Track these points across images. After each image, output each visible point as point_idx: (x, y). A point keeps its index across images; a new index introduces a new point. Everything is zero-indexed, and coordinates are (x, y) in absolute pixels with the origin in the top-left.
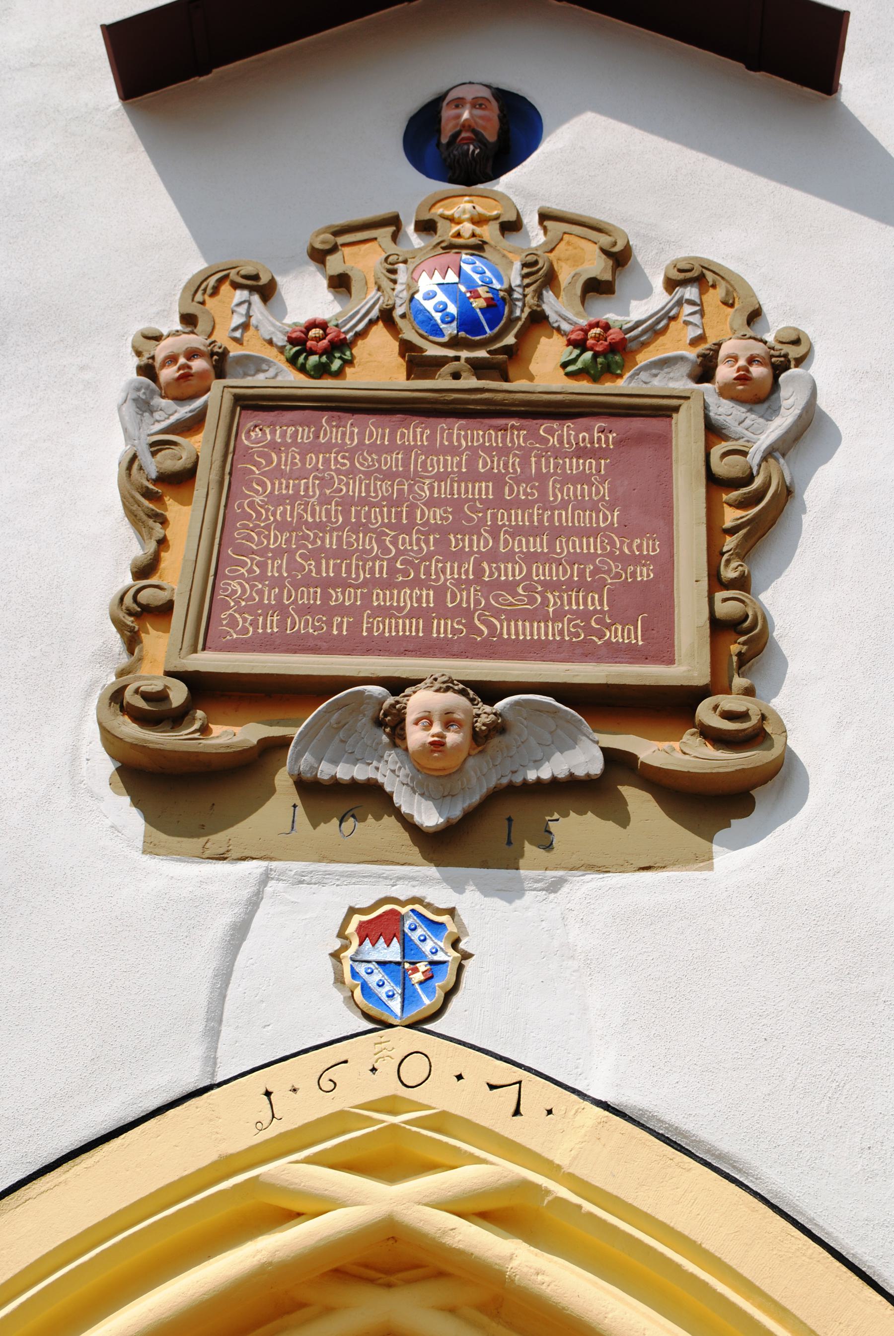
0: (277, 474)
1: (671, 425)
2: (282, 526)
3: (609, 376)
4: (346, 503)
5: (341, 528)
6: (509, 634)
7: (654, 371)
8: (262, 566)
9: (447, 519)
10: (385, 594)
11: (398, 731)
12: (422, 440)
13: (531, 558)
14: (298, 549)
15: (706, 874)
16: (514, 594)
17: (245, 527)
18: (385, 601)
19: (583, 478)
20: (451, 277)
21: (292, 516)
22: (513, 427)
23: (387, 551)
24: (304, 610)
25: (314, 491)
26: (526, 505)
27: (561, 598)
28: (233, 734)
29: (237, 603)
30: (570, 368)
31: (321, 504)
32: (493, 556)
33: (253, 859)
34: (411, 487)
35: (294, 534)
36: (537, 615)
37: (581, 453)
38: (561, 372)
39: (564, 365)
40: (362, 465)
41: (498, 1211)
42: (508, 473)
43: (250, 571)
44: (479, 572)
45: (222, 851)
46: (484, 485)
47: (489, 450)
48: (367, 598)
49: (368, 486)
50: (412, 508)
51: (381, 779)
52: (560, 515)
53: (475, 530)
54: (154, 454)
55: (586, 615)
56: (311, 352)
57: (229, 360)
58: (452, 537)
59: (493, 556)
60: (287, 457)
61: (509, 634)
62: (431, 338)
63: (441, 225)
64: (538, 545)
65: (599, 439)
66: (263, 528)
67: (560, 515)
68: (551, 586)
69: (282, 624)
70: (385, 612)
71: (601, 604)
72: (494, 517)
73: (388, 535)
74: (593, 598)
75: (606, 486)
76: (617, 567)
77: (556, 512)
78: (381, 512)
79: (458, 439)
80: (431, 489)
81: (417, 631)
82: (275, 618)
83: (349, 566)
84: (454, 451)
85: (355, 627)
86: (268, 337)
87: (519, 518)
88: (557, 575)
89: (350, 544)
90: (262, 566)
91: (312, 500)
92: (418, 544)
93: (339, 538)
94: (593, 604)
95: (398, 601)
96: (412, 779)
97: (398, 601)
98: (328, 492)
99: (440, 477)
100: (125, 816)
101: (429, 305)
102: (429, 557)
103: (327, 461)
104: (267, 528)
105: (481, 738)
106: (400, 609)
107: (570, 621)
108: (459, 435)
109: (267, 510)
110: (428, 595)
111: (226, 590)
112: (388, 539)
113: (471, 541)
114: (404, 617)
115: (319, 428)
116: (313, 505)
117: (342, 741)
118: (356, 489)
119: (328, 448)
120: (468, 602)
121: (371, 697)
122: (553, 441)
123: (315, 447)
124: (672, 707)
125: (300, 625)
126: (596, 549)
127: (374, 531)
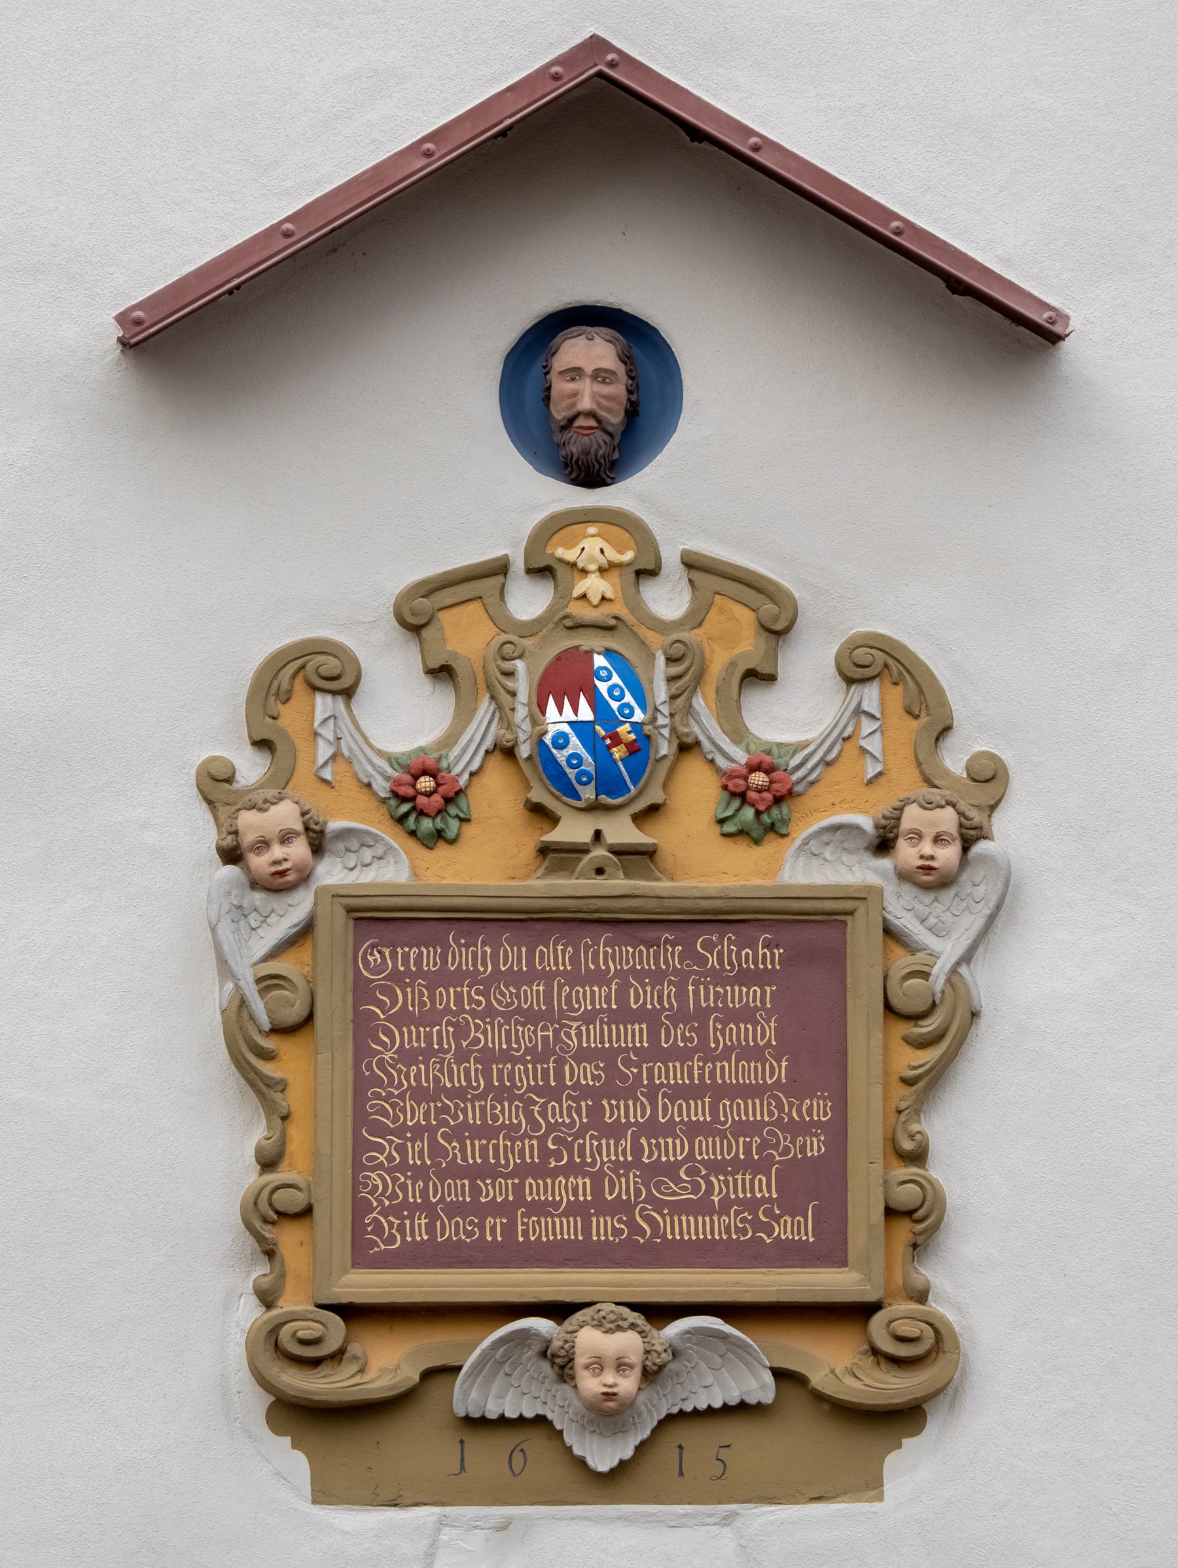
0: (403, 1018)
1: (845, 934)
2: (420, 1094)
3: (772, 836)
4: (487, 1058)
5: (482, 1097)
6: (673, 1233)
7: (825, 838)
8: (402, 1150)
9: (598, 1078)
10: (538, 1185)
11: (567, 1371)
12: (564, 964)
13: (694, 1130)
14: (439, 1126)
15: (876, 1506)
16: (677, 1180)
17: (377, 1096)
18: (538, 1194)
19: (746, 1015)
20: (586, 713)
21: (427, 1081)
22: (667, 941)
23: (535, 1126)
24: (454, 1210)
25: (449, 1043)
26: (683, 1055)
27: (726, 1182)
29: (381, 1203)
30: (729, 828)
31: (459, 1062)
32: (652, 1129)
33: (425, 1504)
34: (556, 1032)
35: (432, 1105)
36: (701, 1207)
37: (744, 978)
38: (716, 829)
39: (722, 822)
40: (500, 1002)
42: (663, 1009)
43: (390, 1158)
44: (637, 1150)
45: (392, 1497)
46: (637, 1027)
47: (640, 975)
48: (519, 1190)
49: (508, 1033)
50: (560, 1062)
51: (550, 1416)
52: (723, 1068)
53: (628, 1094)
54: (262, 992)
55: (752, 1205)
56: (422, 813)
57: (328, 836)
58: (605, 1102)
59: (652, 1129)
60: (413, 993)
61: (673, 1233)
62: (565, 798)
63: (561, 571)
64: (698, 1112)
65: (764, 955)
66: (397, 1097)
67: (723, 1068)
68: (716, 1167)
69: (431, 1229)
70: (540, 1209)
71: (769, 1191)
72: (650, 1070)
73: (536, 1103)
74: (760, 1181)
75: (773, 1025)
76: (785, 1139)
77: (719, 1065)
78: (526, 1069)
79: (606, 963)
80: (579, 1035)
81: (576, 1234)
82: (423, 1221)
83: (496, 1147)
84: (600, 978)
85: (509, 1230)
86: (366, 781)
87: (678, 1073)
88: (722, 1153)
89: (495, 1118)
90: (402, 1150)
91: (449, 1056)
92: (570, 1116)
93: (483, 1109)
94: (761, 1190)
95: (553, 1195)
96: (583, 1417)
97: (553, 1195)
98: (464, 1044)
99: (588, 1018)
100: (288, 1463)
101: (561, 756)
102: (581, 1134)
103: (459, 997)
104: (402, 1096)
105: (650, 1375)
106: (556, 1204)
107: (737, 1213)
108: (606, 953)
109: (399, 1072)
110: (584, 1184)
111: (366, 1185)
112: (536, 1108)
113: (627, 1107)
114: (559, 1216)
115: (446, 948)
116: (450, 1063)
117: (507, 1375)
118: (494, 1038)
119: (457, 978)
120: (628, 1193)
121: (537, 1334)
122: (712, 960)
123: (444, 978)
125: (450, 1230)
126: (762, 1115)
127: (520, 1098)
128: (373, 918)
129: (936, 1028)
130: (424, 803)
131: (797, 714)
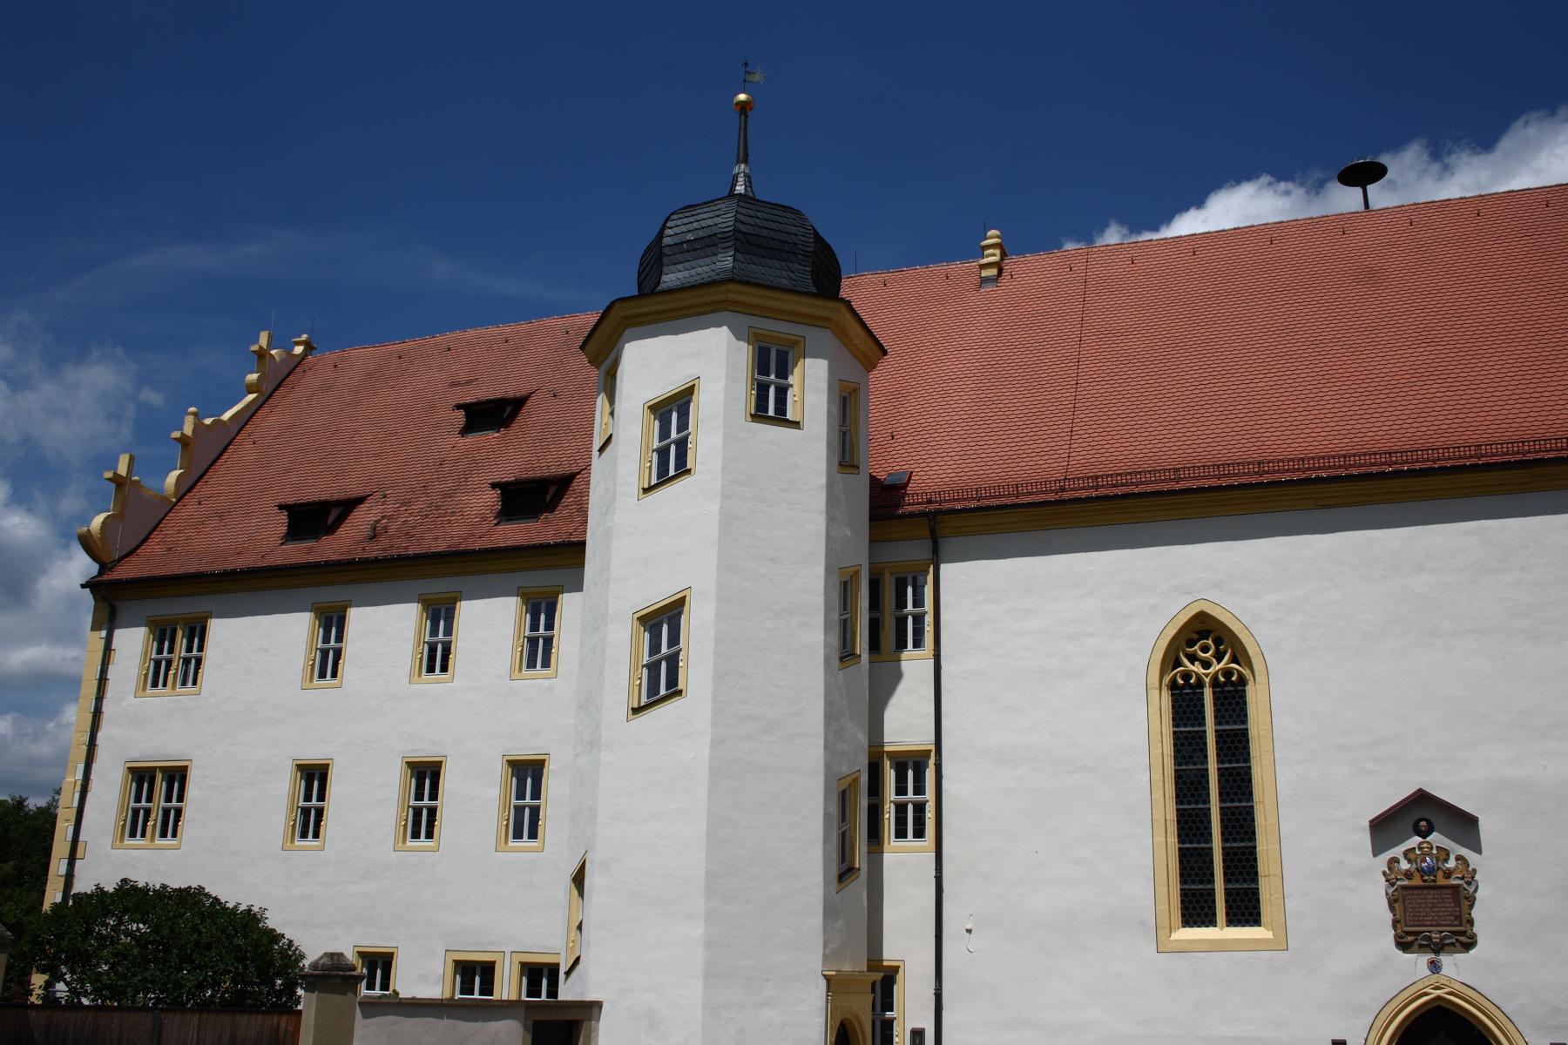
28: (1410, 939)
41: (1450, 993)
124: (1463, 933)
128: (1404, 888)
129: (1471, 901)
130: (1408, 875)
131: (1451, 864)
